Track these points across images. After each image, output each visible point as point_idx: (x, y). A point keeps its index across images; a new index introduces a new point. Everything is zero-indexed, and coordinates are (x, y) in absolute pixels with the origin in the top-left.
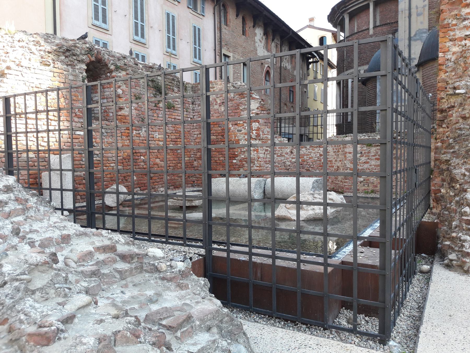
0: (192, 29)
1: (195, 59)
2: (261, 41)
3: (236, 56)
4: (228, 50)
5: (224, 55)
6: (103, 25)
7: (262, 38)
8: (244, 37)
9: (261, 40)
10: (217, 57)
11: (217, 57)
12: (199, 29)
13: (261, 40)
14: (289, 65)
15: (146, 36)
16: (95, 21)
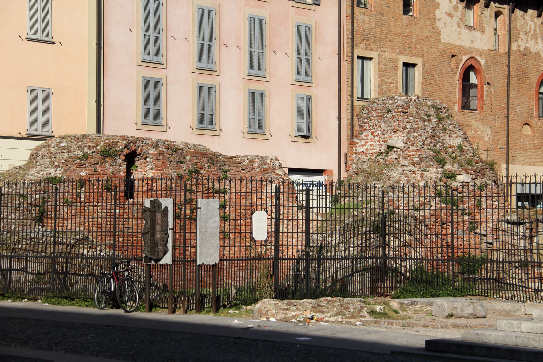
0: (295, 30)
1: (298, 76)
2: (450, 15)
3: (387, 55)
4: (368, 48)
5: (359, 57)
6: (156, 59)
7: (456, 8)
8: (405, 17)
9: (453, 12)
10: (344, 64)
11: (345, 65)
12: (308, 28)
13: (453, 12)
14: (536, 43)
15: (216, 60)
16: (145, 56)
